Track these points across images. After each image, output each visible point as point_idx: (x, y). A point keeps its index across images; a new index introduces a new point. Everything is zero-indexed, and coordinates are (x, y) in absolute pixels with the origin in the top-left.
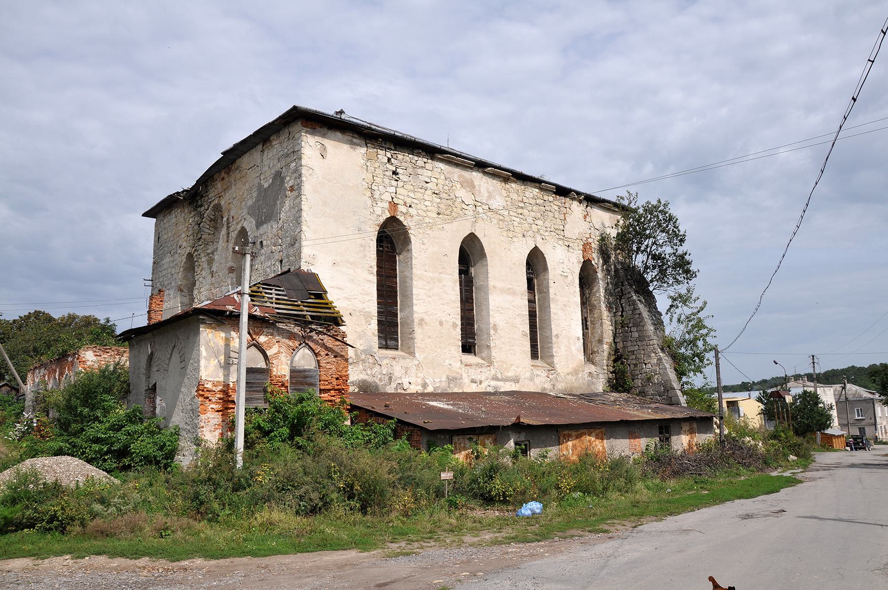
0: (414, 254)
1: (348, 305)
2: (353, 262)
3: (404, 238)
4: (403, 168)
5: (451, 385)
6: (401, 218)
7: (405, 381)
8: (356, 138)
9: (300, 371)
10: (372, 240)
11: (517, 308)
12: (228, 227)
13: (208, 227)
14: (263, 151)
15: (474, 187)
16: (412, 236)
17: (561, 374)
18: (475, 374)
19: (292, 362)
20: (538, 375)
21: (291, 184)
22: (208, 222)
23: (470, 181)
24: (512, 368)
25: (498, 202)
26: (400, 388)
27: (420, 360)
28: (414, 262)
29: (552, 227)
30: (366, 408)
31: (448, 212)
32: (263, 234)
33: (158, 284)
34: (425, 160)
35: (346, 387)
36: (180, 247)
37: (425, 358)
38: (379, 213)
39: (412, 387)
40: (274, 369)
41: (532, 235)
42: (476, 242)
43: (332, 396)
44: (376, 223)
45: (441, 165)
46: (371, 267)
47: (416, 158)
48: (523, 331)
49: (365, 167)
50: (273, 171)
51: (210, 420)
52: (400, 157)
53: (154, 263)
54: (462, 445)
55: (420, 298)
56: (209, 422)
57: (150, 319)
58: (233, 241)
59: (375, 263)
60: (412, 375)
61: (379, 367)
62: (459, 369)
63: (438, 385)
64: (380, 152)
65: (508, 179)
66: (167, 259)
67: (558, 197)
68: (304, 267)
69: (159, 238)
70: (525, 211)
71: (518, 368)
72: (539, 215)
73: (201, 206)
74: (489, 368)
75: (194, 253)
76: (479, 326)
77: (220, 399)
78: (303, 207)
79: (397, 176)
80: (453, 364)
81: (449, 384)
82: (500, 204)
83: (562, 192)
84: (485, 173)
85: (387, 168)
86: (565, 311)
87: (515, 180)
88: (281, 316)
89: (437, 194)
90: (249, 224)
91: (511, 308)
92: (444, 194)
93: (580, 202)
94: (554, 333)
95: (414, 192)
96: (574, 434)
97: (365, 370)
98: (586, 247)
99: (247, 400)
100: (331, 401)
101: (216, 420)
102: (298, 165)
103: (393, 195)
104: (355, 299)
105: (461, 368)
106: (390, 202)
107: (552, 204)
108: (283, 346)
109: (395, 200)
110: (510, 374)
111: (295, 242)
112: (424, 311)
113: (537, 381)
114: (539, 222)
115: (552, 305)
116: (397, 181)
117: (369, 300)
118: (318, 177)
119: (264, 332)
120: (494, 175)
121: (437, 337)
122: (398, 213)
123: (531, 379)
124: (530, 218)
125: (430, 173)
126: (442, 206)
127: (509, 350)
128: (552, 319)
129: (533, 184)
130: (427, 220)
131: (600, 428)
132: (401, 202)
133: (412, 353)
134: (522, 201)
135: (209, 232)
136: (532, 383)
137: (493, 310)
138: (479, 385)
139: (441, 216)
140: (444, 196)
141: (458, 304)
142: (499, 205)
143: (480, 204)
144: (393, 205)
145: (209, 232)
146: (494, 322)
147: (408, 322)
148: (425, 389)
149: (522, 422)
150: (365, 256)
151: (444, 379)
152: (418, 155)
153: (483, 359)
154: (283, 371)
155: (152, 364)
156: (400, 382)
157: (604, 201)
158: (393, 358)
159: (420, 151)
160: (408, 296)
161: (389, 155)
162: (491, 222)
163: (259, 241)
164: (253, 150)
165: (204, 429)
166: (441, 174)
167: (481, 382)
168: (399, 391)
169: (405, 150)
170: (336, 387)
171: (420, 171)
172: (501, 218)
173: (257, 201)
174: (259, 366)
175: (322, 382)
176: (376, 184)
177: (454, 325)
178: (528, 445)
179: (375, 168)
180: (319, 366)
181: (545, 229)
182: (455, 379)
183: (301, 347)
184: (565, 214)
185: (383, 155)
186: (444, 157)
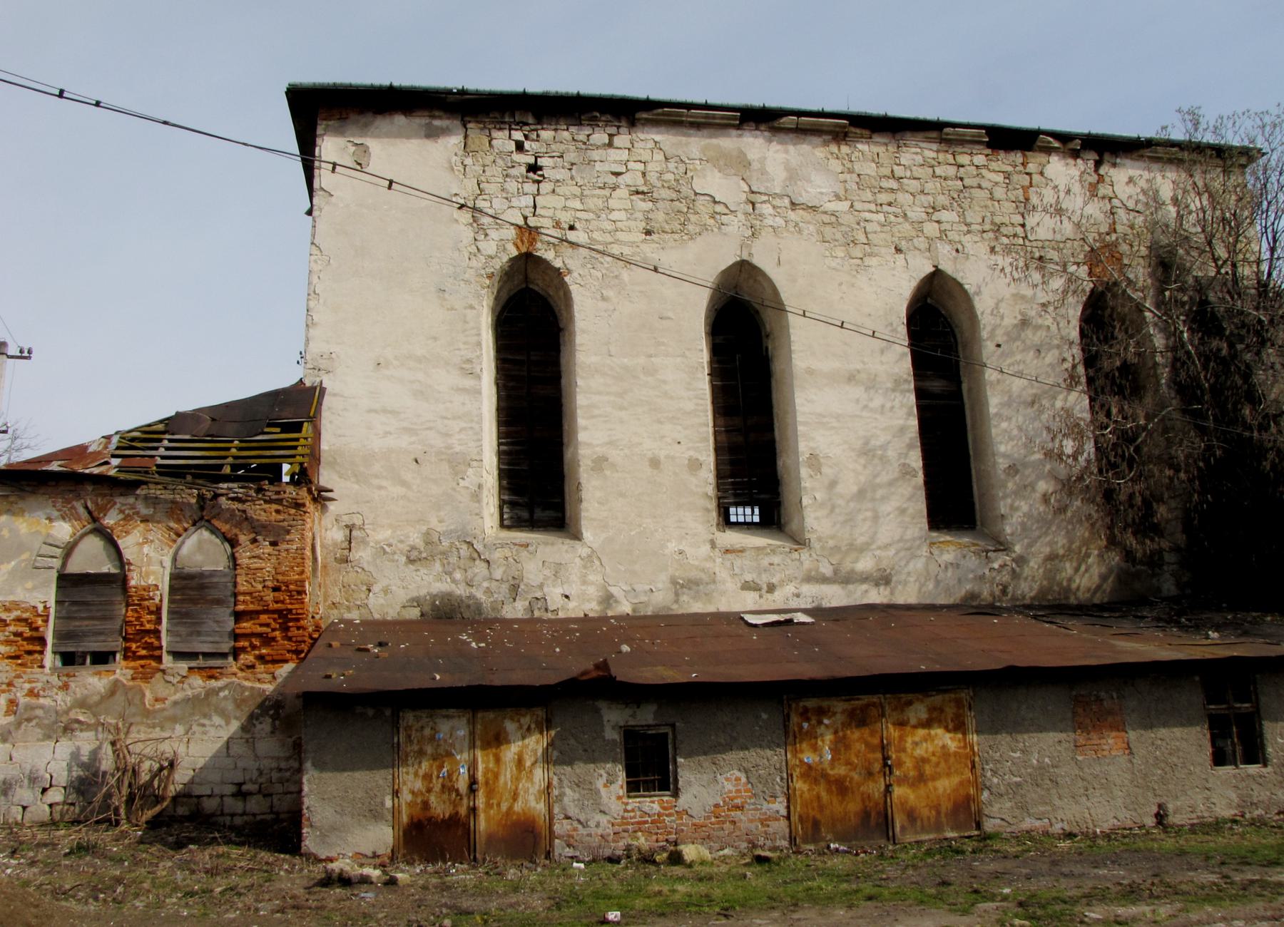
1: (413, 443)
2: (425, 357)
4: (554, 154)
6: (549, 255)
7: (554, 595)
8: (440, 118)
9: (191, 577)
16: (574, 289)
19: (175, 559)
26: (539, 609)
27: (595, 546)
29: (987, 220)
35: (297, 606)
42: (760, 278)
43: (261, 625)
54: (427, 732)
55: (596, 412)
60: (574, 578)
61: (484, 565)
62: (706, 560)
63: (643, 598)
64: (495, 134)
65: (846, 135)
70: (904, 198)
72: (942, 200)
77: (16, 634)
79: (540, 173)
80: (689, 551)
81: (677, 594)
82: (824, 190)
85: (512, 161)
89: (643, 193)
95: (582, 197)
96: (839, 706)
97: (449, 574)
100: (259, 635)
103: (528, 212)
104: (427, 429)
107: (984, 172)
109: (532, 222)
110: (865, 564)
114: (945, 216)
117: (462, 430)
119: (115, 503)
120: (802, 132)
125: (624, 155)
129: (920, 135)
131: (946, 691)
132: (546, 223)
133: (577, 536)
137: (805, 424)
139: (655, 237)
142: (822, 193)
143: (766, 198)
144: (528, 232)
146: (812, 448)
148: (606, 608)
152: (593, 122)
154: (152, 578)
156: (539, 595)
157: (1149, 143)
162: (800, 232)
167: (771, 588)
168: (537, 614)
172: (826, 218)
174: (105, 570)
175: (241, 598)
177: (694, 465)
178: (670, 736)
179: (484, 166)
181: (965, 229)
185: (503, 140)
186: (658, 114)
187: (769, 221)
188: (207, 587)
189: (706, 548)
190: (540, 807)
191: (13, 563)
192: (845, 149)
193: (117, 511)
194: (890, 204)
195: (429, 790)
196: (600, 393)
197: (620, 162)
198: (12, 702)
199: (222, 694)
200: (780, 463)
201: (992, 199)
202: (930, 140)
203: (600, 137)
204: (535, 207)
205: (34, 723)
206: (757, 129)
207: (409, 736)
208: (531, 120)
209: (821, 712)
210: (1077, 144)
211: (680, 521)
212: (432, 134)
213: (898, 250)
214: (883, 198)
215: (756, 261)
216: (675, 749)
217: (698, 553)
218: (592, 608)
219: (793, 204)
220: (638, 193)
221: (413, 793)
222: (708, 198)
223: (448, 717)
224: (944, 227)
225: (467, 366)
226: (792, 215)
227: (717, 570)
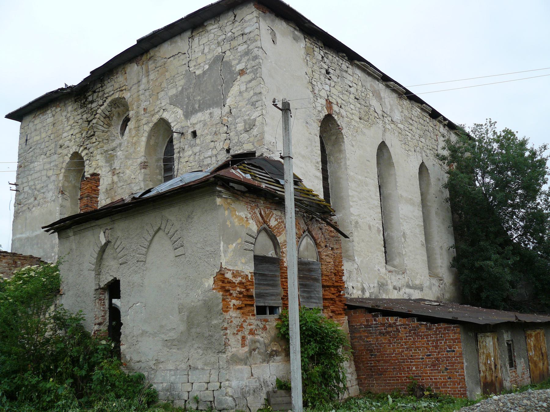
3: (336, 138)
4: (333, 68)
5: (381, 291)
6: (336, 118)
12: (138, 121)
13: (102, 124)
14: (192, 37)
15: (381, 99)
21: (239, 67)
22: (102, 119)
25: (397, 116)
28: (348, 163)
31: (366, 118)
32: (196, 124)
36: (61, 147)
37: (362, 261)
38: (320, 109)
39: (355, 291)
41: (420, 151)
44: (318, 118)
45: (358, 72)
46: (317, 163)
47: (341, 61)
51: (233, 319)
53: (19, 167)
54: (484, 343)
58: (146, 134)
59: (320, 160)
66: (38, 165)
69: (27, 140)
71: (421, 277)
72: (421, 133)
73: (92, 102)
75: (82, 152)
77: (240, 293)
80: (381, 269)
81: (379, 290)
83: (434, 115)
84: (388, 86)
89: (357, 99)
93: (444, 126)
95: (343, 94)
101: (238, 319)
105: (386, 274)
110: (417, 282)
116: (329, 79)
118: (271, 62)
119: (273, 214)
120: (394, 91)
121: (368, 241)
122: (334, 112)
125: (351, 78)
126: (362, 111)
134: (411, 119)
135: (103, 129)
136: (431, 291)
138: (399, 292)
139: (362, 121)
143: (386, 115)
145: (103, 129)
151: (376, 285)
153: (394, 266)
155: (105, 256)
163: (191, 130)
164: (178, 39)
165: (228, 331)
170: (336, 284)
176: (315, 80)
185: (318, 53)
186: (362, 64)
188: (311, 271)
191: (234, 245)
192: (401, 103)
193: (274, 220)
194: (411, 130)
195: (486, 370)
198: (243, 338)
204: (330, 92)
205: (256, 352)
206: (382, 84)
207: (480, 345)
209: (531, 335)
210: (446, 122)
211: (377, 256)
215: (386, 142)
216: (513, 349)
217: (383, 270)
219: (392, 120)
220: (356, 98)
223: (488, 336)
226: (393, 126)
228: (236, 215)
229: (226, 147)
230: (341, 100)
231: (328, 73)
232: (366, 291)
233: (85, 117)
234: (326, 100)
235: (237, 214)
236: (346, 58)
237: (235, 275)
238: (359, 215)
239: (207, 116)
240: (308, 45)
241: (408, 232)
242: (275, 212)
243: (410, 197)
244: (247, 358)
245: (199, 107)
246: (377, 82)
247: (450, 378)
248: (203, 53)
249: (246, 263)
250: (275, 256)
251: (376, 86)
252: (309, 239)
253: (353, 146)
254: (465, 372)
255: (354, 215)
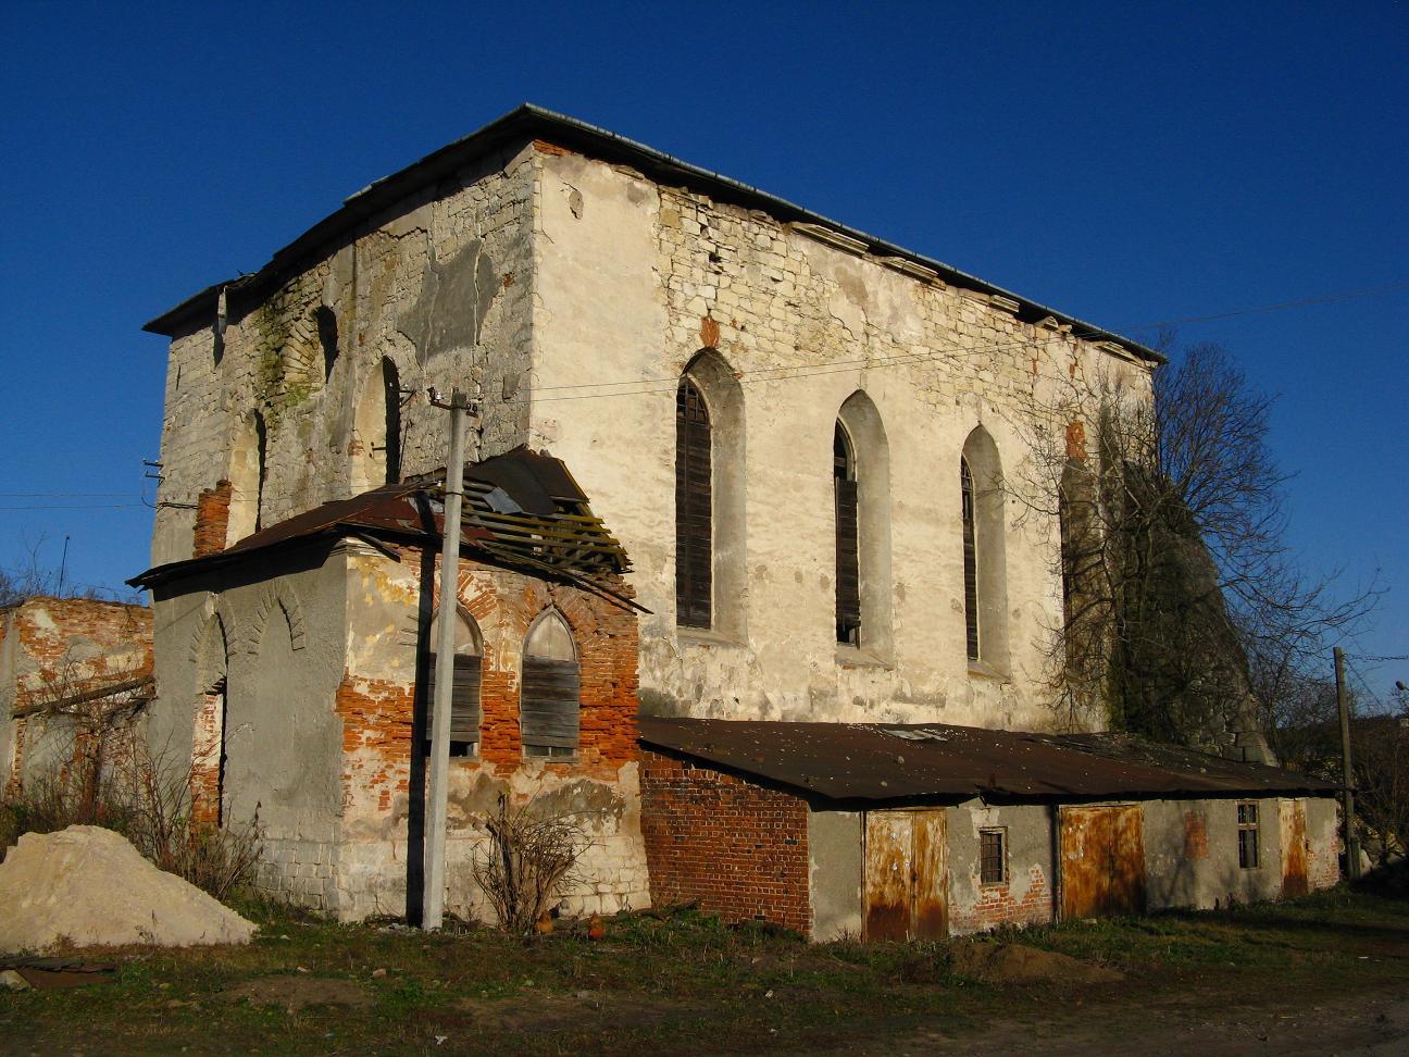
0: (750, 430)
3: (729, 394)
5: (816, 708)
6: (726, 353)
10: (670, 397)
11: (943, 552)
13: (298, 356)
17: (1024, 692)
18: (858, 683)
19: (526, 645)
20: (979, 693)
21: (506, 269)
23: (857, 281)
24: (933, 677)
25: (911, 329)
27: (758, 652)
28: (750, 445)
29: (1011, 386)
30: (671, 747)
31: (815, 345)
33: (176, 475)
34: (773, 234)
37: (767, 648)
39: (740, 708)
40: (492, 659)
46: (666, 452)
47: (755, 229)
48: (953, 600)
49: (657, 241)
50: (462, 243)
52: (725, 225)
54: (885, 832)
55: (760, 521)
56: (361, 766)
57: (199, 542)
59: (674, 444)
63: (790, 706)
67: (1022, 323)
68: (535, 446)
69: (179, 377)
71: (943, 676)
72: (985, 360)
73: (283, 311)
74: (887, 675)
76: (866, 586)
78: (535, 320)
79: (719, 264)
82: (913, 333)
86: (1031, 561)
87: (942, 283)
88: (510, 547)
90: (403, 355)
91: (933, 551)
92: (809, 308)
94: (1012, 606)
95: (751, 299)
97: (652, 670)
98: (1073, 434)
99: (454, 722)
102: (526, 230)
105: (834, 673)
106: (704, 319)
108: (510, 612)
110: (928, 689)
111: (514, 389)
112: (767, 549)
113: (979, 704)
114: (985, 375)
115: (1009, 549)
116: (717, 273)
117: (660, 523)
118: (565, 258)
119: (472, 578)
121: (790, 606)
122: (720, 342)
123: (968, 701)
124: (969, 365)
125: (781, 263)
126: (804, 331)
127: (927, 638)
128: (1008, 576)
130: (775, 359)
133: (738, 642)
136: (968, 709)
137: (896, 554)
138: (869, 711)
140: (808, 310)
141: (832, 539)
144: (710, 326)
147: (728, 570)
149: (1000, 789)
150: (654, 429)
156: (717, 697)
158: (704, 647)
159: (764, 214)
160: (729, 519)
161: (703, 219)
163: (426, 387)
165: (351, 782)
166: (804, 265)
167: (871, 706)
168: (716, 716)
169: (734, 212)
171: (762, 256)
173: (422, 304)
177: (824, 582)
180: (581, 655)
182: (823, 694)
183: (545, 613)
184: (1034, 361)
185: (691, 221)
186: (811, 229)
187: (877, 355)
188: (556, 679)
189: (831, 664)
190: (941, 894)
191: (378, 636)
193: (474, 588)
195: (885, 883)
196: (760, 502)
197: (778, 269)
199: (575, 792)
200: (860, 586)
201: (1014, 366)
202: (981, 301)
203: (763, 240)
204: (716, 300)
208: (710, 204)
211: (814, 635)
212: (635, 198)
213: (957, 403)
214: (950, 349)
218: (754, 714)
221: (874, 885)
222: (840, 323)
224: (986, 386)
225: (665, 457)
226: (894, 353)
227: (839, 684)
228: (386, 584)
229: (478, 427)
230: (744, 313)
231: (714, 258)
232: (772, 708)
233: (270, 339)
234: (704, 319)
235: (389, 582)
236: (770, 219)
237: (373, 687)
238: (770, 553)
239: (452, 359)
240: (668, 205)
241: (912, 583)
242: (476, 574)
243: (927, 506)
244: (389, 829)
245: (440, 343)
246: (857, 260)
247: (786, 892)
248: (453, 233)
249: (401, 667)
250: (471, 653)
251: (852, 272)
252: (555, 621)
253: (768, 409)
254: (811, 883)
255: (754, 552)
